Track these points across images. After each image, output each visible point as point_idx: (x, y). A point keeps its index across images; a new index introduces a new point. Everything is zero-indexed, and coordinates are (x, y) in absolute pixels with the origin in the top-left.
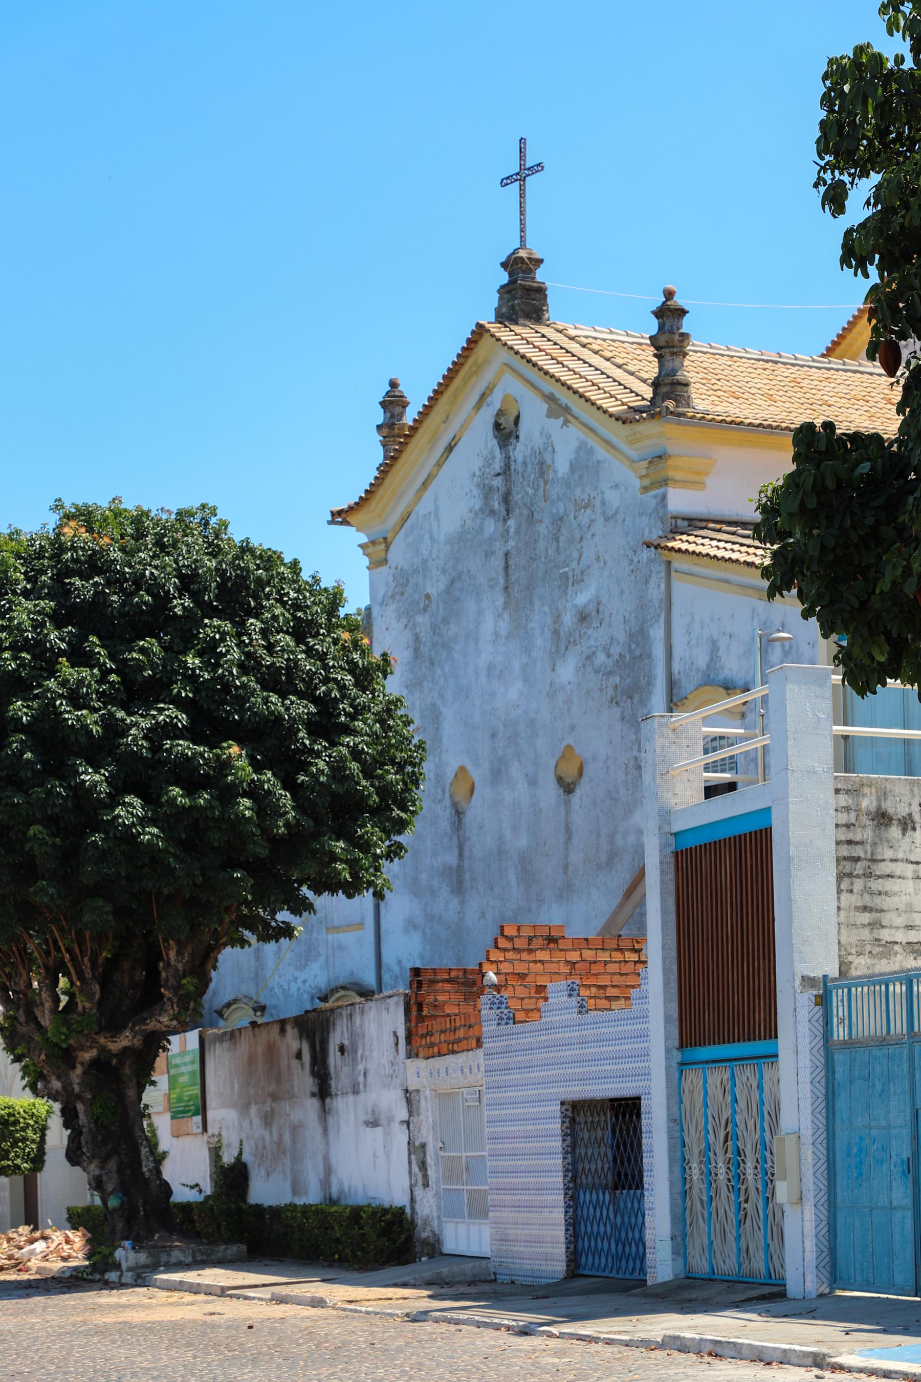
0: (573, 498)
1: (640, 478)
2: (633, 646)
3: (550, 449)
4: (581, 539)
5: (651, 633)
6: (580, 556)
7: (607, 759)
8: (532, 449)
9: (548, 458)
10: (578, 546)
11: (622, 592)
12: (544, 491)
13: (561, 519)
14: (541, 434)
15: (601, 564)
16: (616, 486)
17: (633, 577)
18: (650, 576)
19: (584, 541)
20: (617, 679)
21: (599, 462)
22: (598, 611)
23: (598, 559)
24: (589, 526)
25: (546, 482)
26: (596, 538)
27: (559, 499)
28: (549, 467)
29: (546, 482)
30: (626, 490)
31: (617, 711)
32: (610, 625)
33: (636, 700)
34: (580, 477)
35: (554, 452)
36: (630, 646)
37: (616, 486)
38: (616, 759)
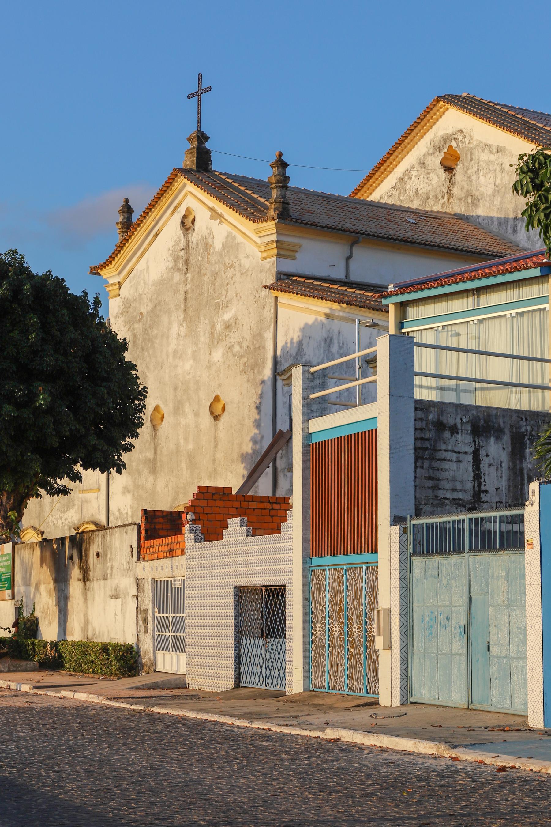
0: (223, 262)
1: (261, 252)
2: (255, 342)
3: (211, 236)
4: (228, 284)
5: (265, 335)
6: (227, 294)
7: (239, 403)
8: (201, 236)
9: (210, 241)
10: (226, 288)
11: (249, 313)
12: (208, 258)
13: (216, 274)
14: (207, 228)
15: (239, 298)
16: (248, 257)
17: (256, 305)
18: (265, 305)
19: (229, 286)
20: (246, 360)
21: (238, 243)
22: (236, 323)
23: (237, 295)
24: (232, 278)
25: (209, 254)
26: (235, 284)
27: (216, 263)
28: (211, 246)
29: (209, 254)
30: (253, 258)
31: (245, 377)
32: (242, 331)
33: (255, 371)
34: (228, 251)
35: (213, 238)
36: (253, 342)
37: (248, 257)
38: (244, 403)
